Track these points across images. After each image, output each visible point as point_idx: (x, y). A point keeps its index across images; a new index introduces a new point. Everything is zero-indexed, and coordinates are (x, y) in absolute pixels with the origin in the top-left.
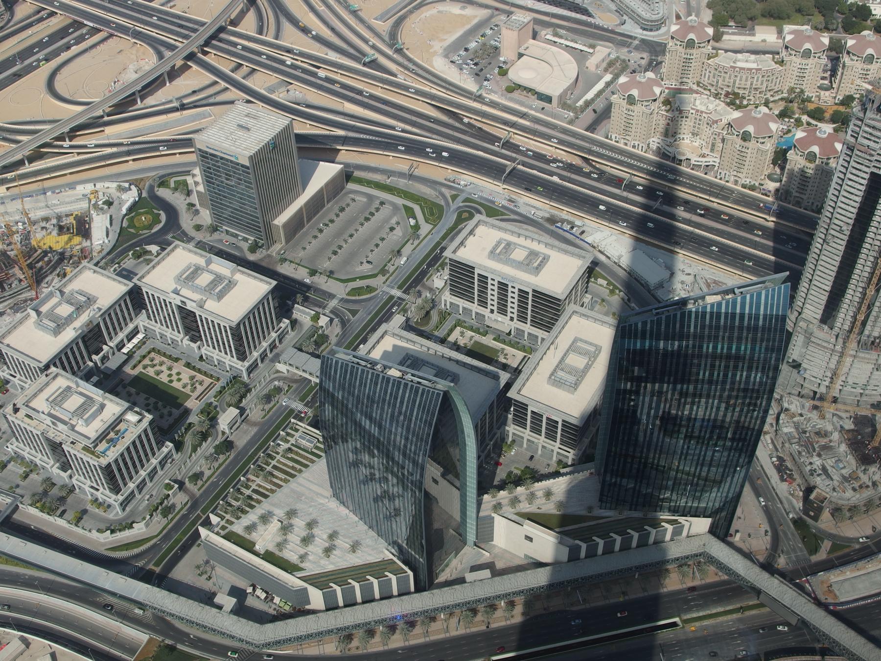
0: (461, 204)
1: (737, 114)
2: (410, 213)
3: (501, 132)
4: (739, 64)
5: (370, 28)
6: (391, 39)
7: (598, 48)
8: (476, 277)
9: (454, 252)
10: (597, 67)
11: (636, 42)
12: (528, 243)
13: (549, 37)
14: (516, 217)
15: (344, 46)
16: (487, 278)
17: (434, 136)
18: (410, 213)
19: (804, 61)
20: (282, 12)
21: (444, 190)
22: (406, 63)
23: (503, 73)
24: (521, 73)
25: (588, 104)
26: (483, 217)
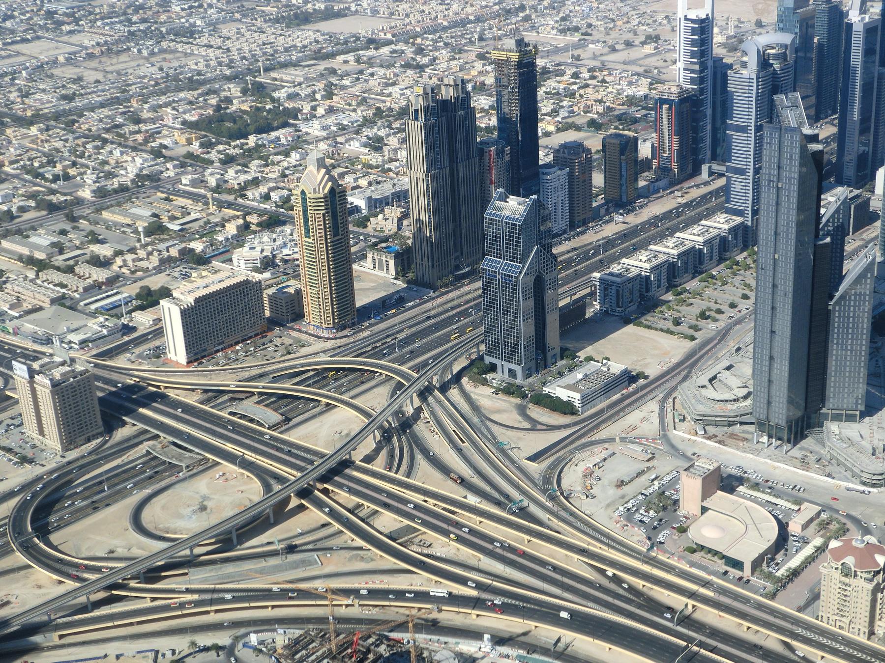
3: (676, 601)
5: (520, 469)
6: (544, 483)
10: (805, 527)
15: (488, 489)
17: (590, 604)
20: (417, 446)
22: (563, 514)
23: (683, 530)
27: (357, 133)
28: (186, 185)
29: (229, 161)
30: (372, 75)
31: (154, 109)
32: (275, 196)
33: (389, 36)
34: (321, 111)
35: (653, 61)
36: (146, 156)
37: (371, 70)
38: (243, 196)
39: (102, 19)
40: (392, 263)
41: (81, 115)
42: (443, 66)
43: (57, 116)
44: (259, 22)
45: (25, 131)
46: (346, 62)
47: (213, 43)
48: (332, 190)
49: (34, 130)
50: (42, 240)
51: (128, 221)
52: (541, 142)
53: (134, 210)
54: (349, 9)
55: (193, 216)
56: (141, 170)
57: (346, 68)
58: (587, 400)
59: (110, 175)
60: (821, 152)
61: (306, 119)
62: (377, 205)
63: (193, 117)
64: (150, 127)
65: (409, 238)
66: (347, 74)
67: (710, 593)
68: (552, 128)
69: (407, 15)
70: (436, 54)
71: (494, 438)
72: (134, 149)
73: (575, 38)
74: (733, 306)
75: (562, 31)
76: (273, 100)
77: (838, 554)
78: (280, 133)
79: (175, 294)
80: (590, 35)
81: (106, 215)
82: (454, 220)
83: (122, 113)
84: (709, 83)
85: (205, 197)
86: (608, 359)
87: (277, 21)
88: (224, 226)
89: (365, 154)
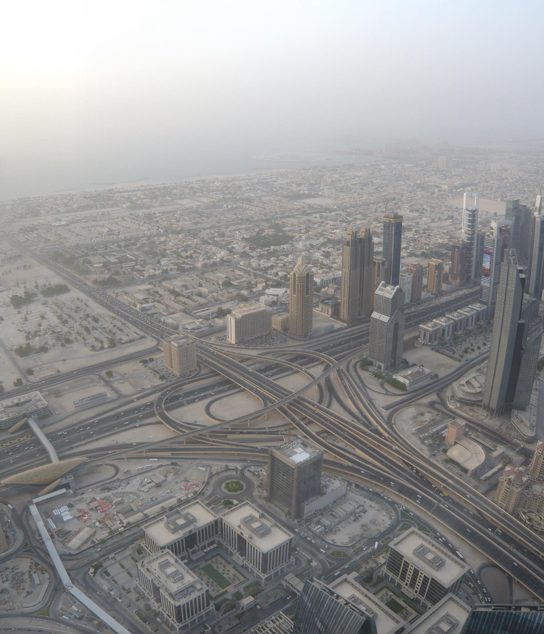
29: (261, 256)
30: (327, 224)
32: (280, 274)
33: (335, 207)
34: (303, 238)
36: (226, 251)
38: (267, 273)
42: (358, 222)
55: (244, 279)
57: (315, 220)
59: (209, 258)
61: (297, 241)
62: (325, 284)
64: (228, 239)
69: (344, 199)
72: (221, 248)
76: (283, 231)
78: (285, 246)
81: (206, 275)
83: (217, 232)
85: (249, 271)
88: (256, 285)
89: (321, 259)
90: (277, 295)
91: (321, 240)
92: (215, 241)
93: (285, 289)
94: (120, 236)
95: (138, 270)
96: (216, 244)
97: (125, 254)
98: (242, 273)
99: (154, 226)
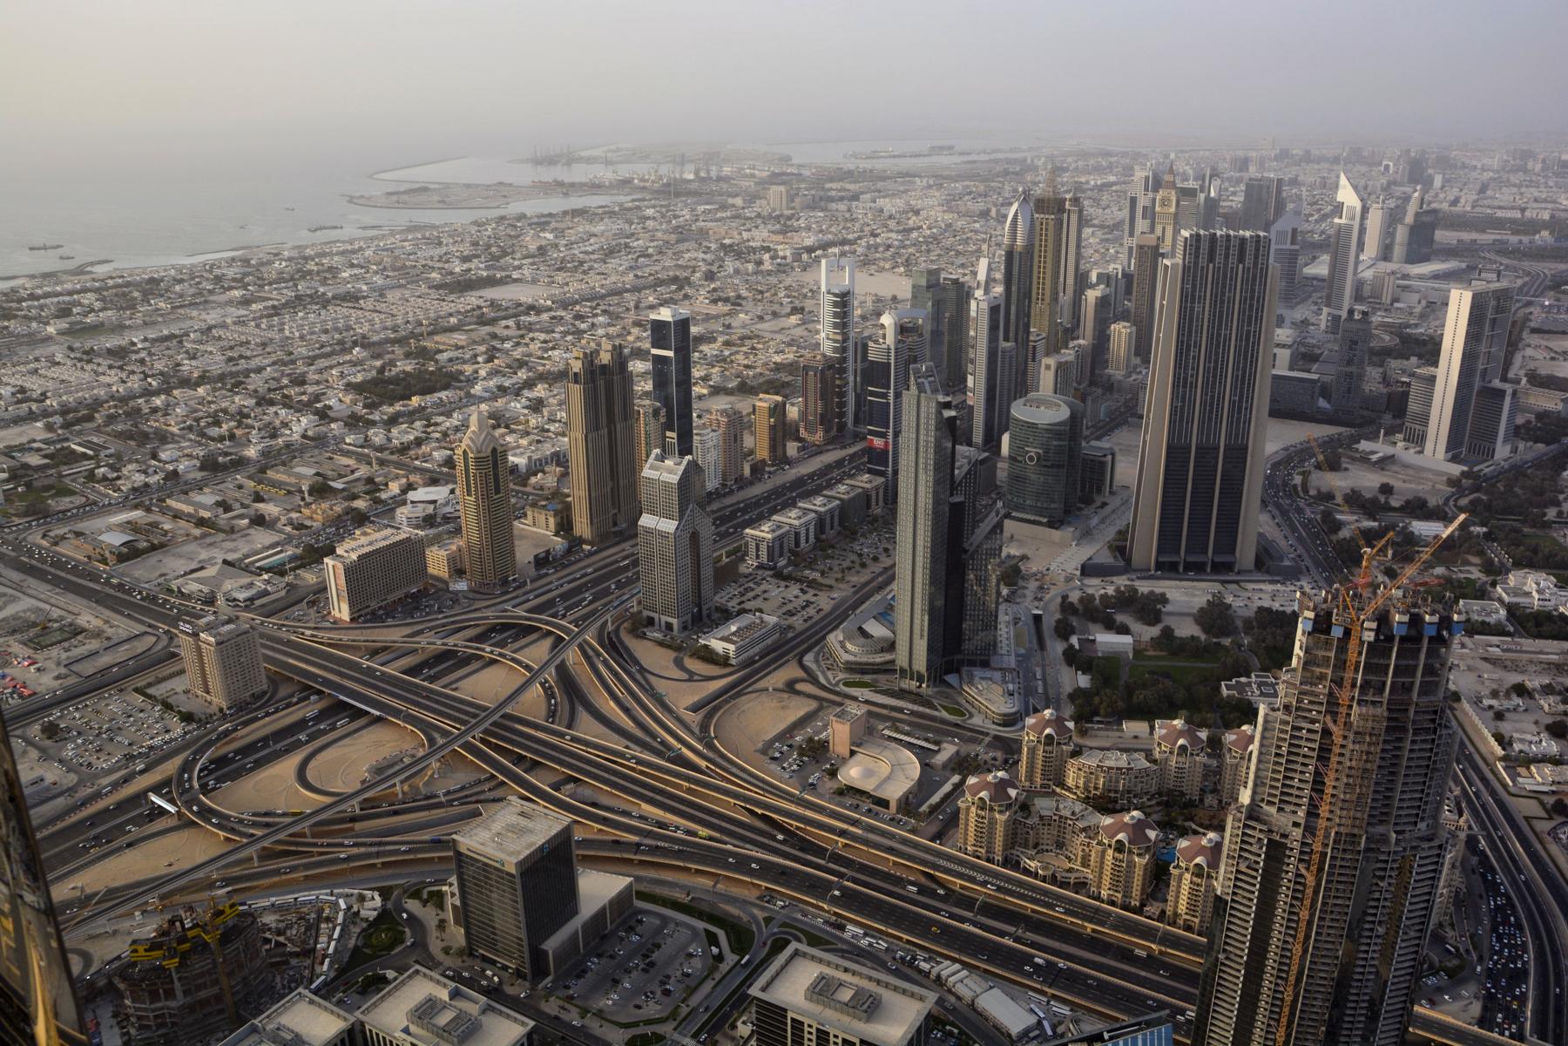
0: (776, 930)
1: (1108, 821)
2: (712, 939)
4: (1108, 763)
5: (679, 720)
6: (701, 732)
7: (945, 745)
8: (789, 1021)
9: (764, 989)
11: (988, 739)
12: (855, 980)
13: (886, 732)
14: (844, 947)
16: (802, 1024)
17: (747, 846)
18: (712, 939)
19: (1182, 759)
21: (756, 911)
22: (719, 760)
23: (833, 773)
24: (852, 774)
25: (934, 809)
26: (803, 947)
27: (517, 395)
28: (350, 444)
29: (393, 421)
30: (532, 339)
31: (320, 372)
33: (549, 303)
34: (483, 373)
35: (799, 332)
37: (531, 335)
39: (270, 284)
40: (552, 521)
41: (247, 376)
42: (601, 332)
43: (222, 378)
44: (423, 288)
45: (192, 392)
46: (507, 327)
47: (378, 308)
48: (494, 450)
49: (201, 391)
50: (208, 498)
51: (293, 480)
52: (695, 406)
53: (298, 470)
54: (510, 277)
55: (357, 475)
56: (306, 431)
57: (506, 332)
58: (739, 651)
59: (274, 436)
60: (954, 418)
62: (536, 467)
63: (359, 378)
64: (315, 388)
65: (569, 496)
66: (508, 339)
67: (860, 832)
68: (705, 391)
69: (567, 284)
70: (595, 320)
71: (653, 689)
73: (722, 308)
74: (875, 559)
75: (714, 302)
76: (437, 361)
77: (976, 790)
78: (443, 395)
79: (339, 551)
80: (740, 305)
81: (270, 474)
82: (612, 479)
83: (288, 375)
84: (850, 353)
85: (368, 456)
86: (761, 611)
87: (438, 287)
88: (386, 485)
89: (525, 415)
90: (434, 502)
91: (523, 375)
92: (285, 396)
93: (451, 486)
94: (48, 402)
95: (105, 478)
96: (287, 402)
97: (65, 445)
98: (351, 462)
99: (133, 372)
